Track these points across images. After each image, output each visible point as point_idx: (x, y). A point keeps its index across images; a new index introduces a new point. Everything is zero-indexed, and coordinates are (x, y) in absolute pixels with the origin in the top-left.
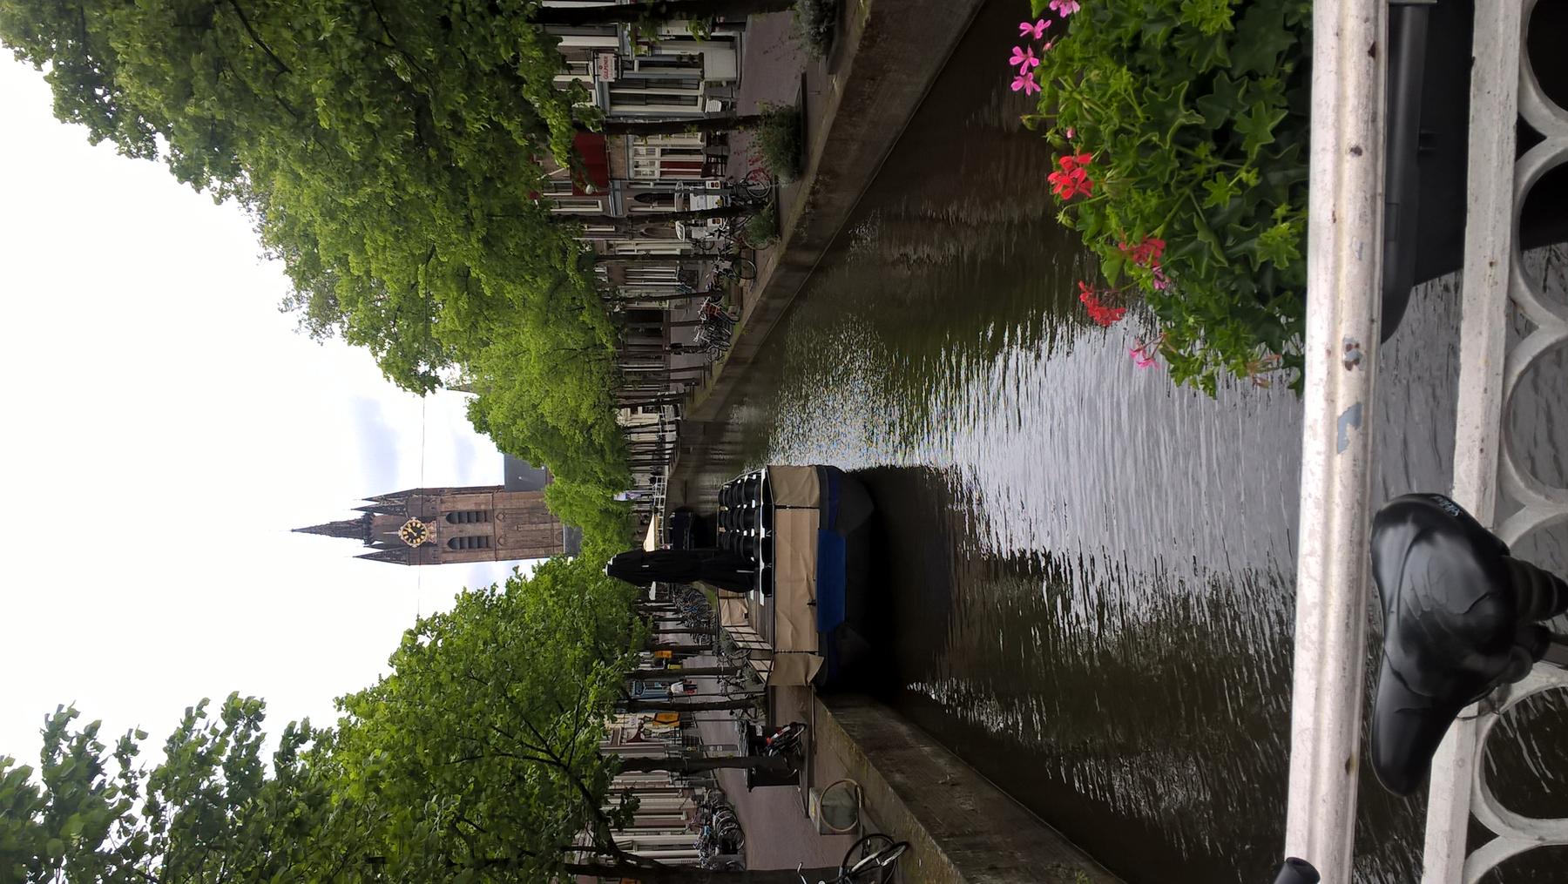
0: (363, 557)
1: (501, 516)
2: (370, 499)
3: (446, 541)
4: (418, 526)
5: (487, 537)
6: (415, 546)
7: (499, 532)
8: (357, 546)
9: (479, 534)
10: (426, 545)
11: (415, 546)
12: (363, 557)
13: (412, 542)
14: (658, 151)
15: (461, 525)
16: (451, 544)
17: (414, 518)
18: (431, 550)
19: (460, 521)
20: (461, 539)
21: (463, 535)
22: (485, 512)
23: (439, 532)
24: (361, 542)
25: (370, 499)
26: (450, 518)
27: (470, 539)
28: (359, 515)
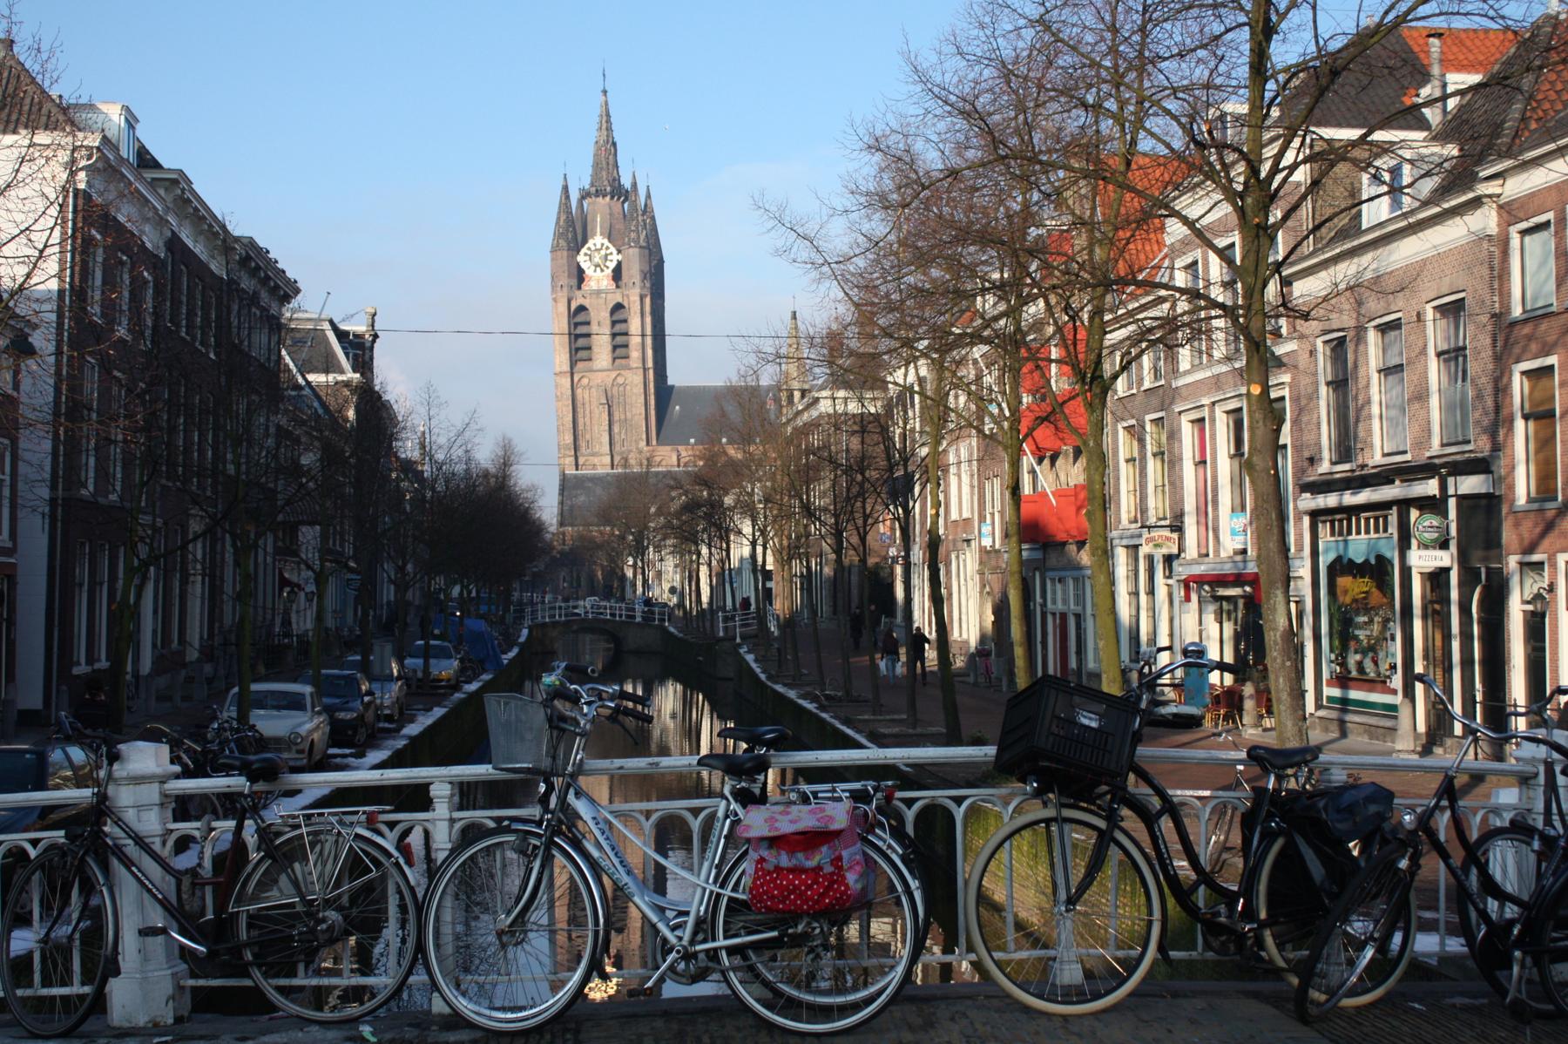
0: (566, 189)
1: (620, 380)
2: (648, 196)
3: (586, 303)
4: (608, 263)
7: (598, 378)
8: (581, 178)
9: (595, 349)
10: (580, 276)
12: (566, 189)
13: (586, 254)
14: (1079, 609)
15: (608, 322)
18: (574, 282)
19: (614, 323)
21: (594, 328)
22: (627, 357)
23: (598, 292)
24: (586, 183)
25: (648, 196)
26: (618, 307)
28: (626, 182)
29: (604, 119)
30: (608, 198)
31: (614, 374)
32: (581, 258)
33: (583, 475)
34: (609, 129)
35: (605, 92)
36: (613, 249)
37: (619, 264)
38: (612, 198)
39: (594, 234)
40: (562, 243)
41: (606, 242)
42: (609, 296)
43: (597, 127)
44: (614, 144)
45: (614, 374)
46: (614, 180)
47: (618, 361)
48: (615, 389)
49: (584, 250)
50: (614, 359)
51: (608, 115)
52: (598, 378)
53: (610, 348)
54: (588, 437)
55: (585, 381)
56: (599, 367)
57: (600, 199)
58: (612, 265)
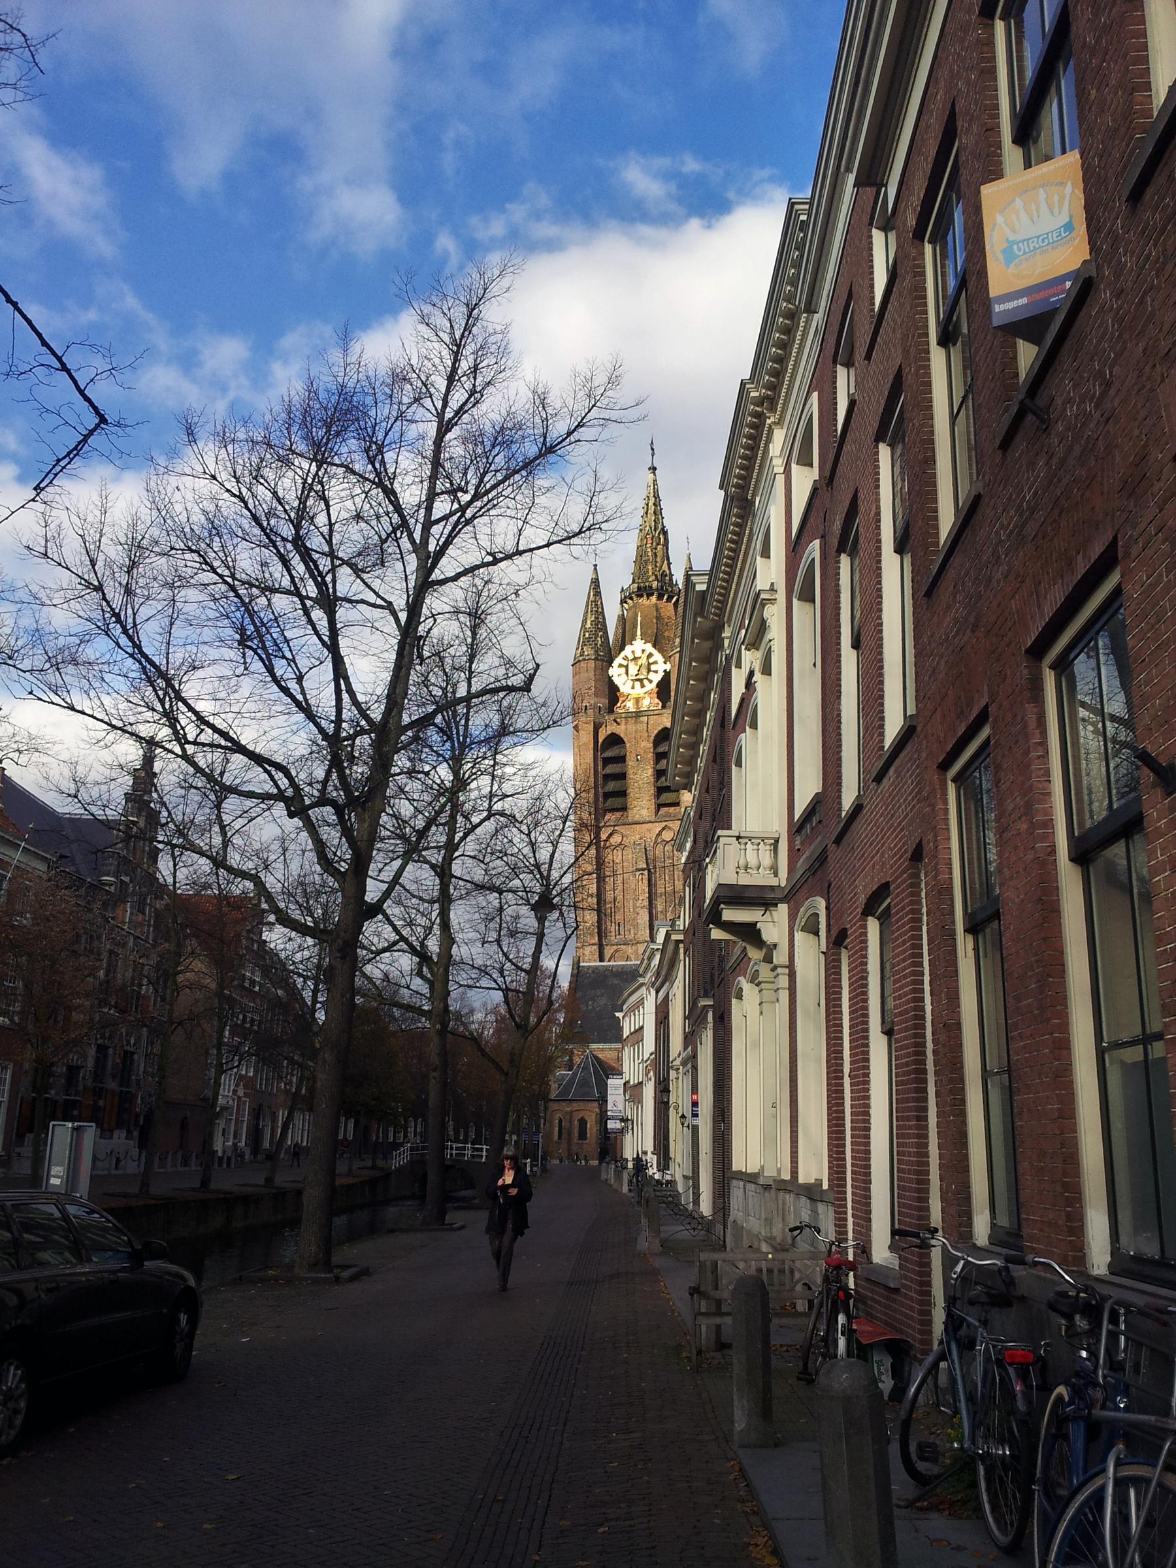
3: (620, 730)
4: (652, 676)
5: (624, 809)
6: (611, 672)
9: (632, 792)
10: (613, 693)
11: (611, 672)
12: (595, 582)
13: (620, 666)
16: (615, 740)
17: (668, 667)
18: (603, 702)
20: (622, 759)
21: (631, 762)
23: (638, 714)
24: (626, 581)
27: (622, 776)
29: (652, 500)
30: (654, 599)
31: (657, 827)
32: (615, 672)
33: (606, 968)
34: (658, 512)
35: (653, 469)
36: (658, 656)
37: (667, 674)
38: (660, 597)
39: (633, 638)
40: (588, 651)
41: (649, 648)
42: (652, 720)
43: (642, 512)
44: (665, 533)
45: (657, 827)
46: (664, 575)
47: (663, 811)
48: (660, 847)
49: (618, 660)
50: (659, 806)
51: (657, 496)
52: (634, 835)
53: (652, 791)
54: (619, 917)
55: (616, 839)
56: (637, 818)
57: (644, 601)
58: (657, 678)
